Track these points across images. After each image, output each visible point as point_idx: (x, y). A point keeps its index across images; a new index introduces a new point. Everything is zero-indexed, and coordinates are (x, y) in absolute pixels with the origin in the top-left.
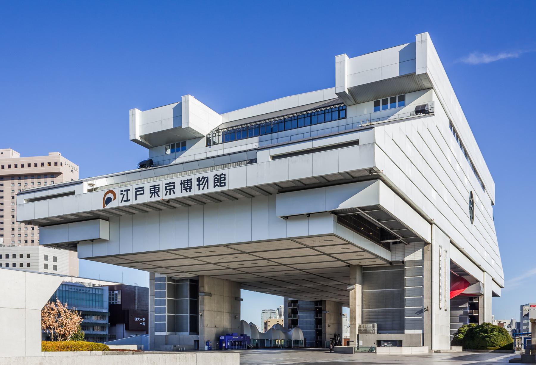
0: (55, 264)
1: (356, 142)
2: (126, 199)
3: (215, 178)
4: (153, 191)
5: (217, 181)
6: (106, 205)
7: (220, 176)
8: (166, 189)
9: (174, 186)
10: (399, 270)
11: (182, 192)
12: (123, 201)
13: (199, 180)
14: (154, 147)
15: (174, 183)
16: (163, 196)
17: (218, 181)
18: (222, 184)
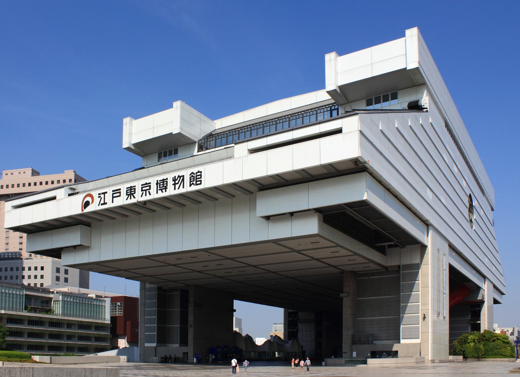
0: (66, 276)
1: (339, 131)
2: (103, 203)
3: (191, 176)
4: (130, 193)
5: (193, 180)
6: (85, 209)
7: (196, 174)
8: (142, 190)
9: (150, 186)
10: (395, 275)
11: (157, 193)
12: (100, 204)
13: (174, 180)
14: (147, 155)
15: (150, 183)
16: (139, 197)
17: (194, 179)
18: (198, 183)
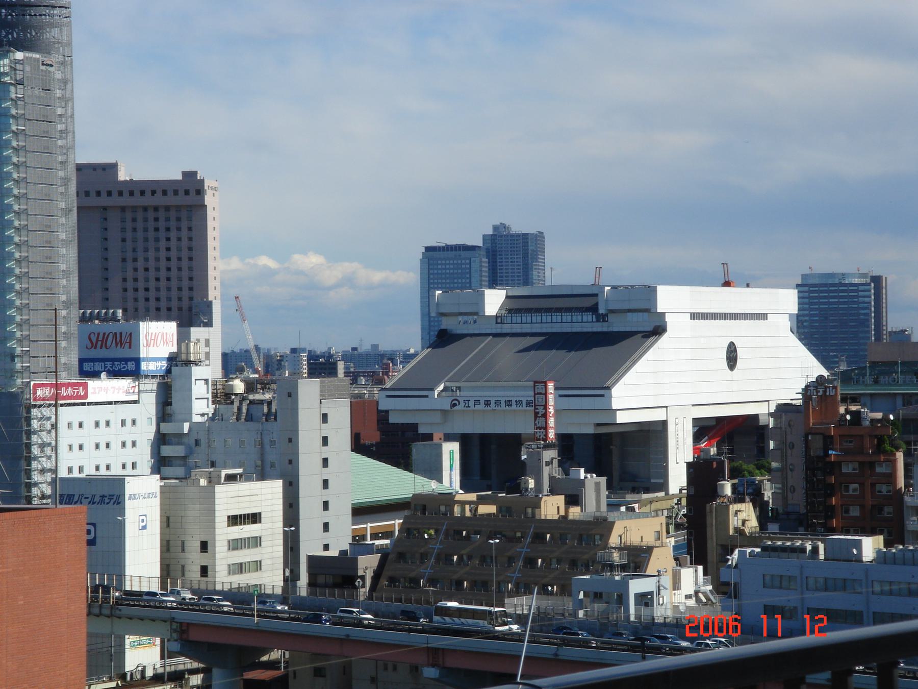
13: (516, 401)
